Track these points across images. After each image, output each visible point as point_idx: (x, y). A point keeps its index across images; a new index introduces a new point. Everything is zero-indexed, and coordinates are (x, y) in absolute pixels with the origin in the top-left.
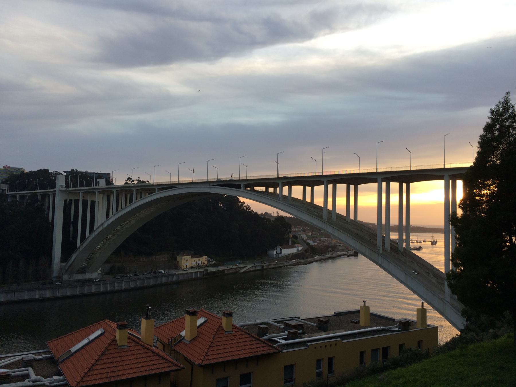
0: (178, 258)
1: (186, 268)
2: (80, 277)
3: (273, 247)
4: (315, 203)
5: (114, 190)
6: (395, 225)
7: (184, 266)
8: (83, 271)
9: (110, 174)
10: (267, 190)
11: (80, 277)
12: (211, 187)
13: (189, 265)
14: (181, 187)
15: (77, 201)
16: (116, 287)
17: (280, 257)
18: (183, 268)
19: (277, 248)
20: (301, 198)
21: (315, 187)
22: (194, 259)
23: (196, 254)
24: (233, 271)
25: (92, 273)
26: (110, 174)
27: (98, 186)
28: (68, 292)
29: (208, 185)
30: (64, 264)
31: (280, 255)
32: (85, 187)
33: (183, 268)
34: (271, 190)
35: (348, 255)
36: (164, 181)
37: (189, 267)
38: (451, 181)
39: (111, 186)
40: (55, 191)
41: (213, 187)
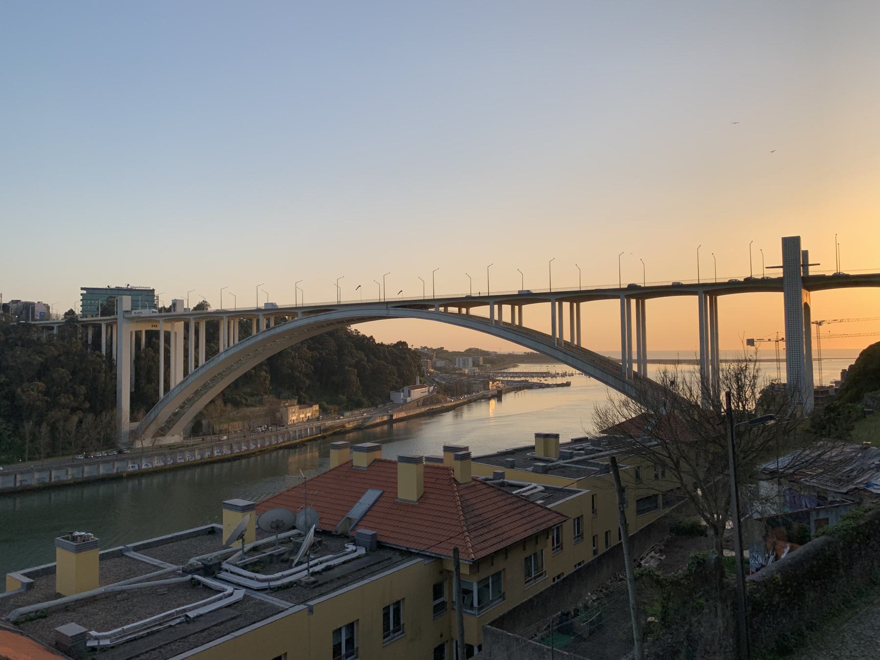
3: (397, 389)
4: (524, 325)
5: (225, 316)
6: (525, 353)
8: (162, 432)
9: (153, 290)
10: (460, 310)
12: (390, 308)
17: (410, 402)
19: (403, 390)
20: (510, 321)
21: (523, 306)
23: (303, 403)
24: (354, 425)
25: (173, 436)
26: (153, 290)
27: (174, 311)
28: (157, 463)
29: (384, 306)
30: (136, 425)
31: (409, 399)
34: (464, 311)
35: (490, 396)
36: (319, 302)
38: (708, 297)
39: (205, 311)
40: (116, 319)
41: (393, 308)
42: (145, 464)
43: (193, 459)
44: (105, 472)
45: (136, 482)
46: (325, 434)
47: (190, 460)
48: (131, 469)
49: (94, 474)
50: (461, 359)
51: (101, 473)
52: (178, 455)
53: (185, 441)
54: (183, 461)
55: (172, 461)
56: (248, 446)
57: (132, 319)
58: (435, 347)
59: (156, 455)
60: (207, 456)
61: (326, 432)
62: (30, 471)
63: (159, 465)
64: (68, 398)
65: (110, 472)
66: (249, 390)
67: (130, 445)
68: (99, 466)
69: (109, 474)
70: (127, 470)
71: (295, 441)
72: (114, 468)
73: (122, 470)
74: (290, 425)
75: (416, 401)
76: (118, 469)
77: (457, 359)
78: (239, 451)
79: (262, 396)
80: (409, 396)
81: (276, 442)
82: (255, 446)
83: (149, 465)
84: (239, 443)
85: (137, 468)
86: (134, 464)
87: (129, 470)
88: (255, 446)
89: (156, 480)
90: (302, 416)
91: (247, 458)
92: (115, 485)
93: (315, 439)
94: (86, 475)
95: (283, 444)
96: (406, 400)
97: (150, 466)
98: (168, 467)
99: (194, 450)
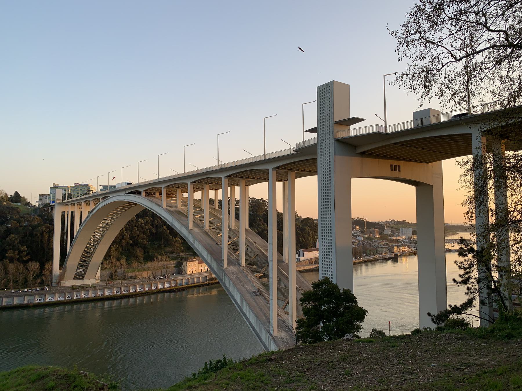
0: (184, 263)
1: (192, 273)
2: (79, 283)
7: (189, 272)
8: (80, 276)
11: (79, 283)
13: (196, 271)
14: (111, 195)
15: (68, 212)
16: (107, 293)
18: (188, 273)
22: (201, 264)
31: (302, 259)
32: (68, 199)
33: (188, 273)
37: (196, 272)
42: (49, 298)
43: (88, 297)
44: (20, 302)
45: (42, 310)
46: (211, 282)
47: (86, 297)
48: (39, 301)
49: (11, 303)
50: (403, 229)
51: (15, 303)
52: (75, 293)
53: (102, 283)
54: (79, 297)
55: (71, 298)
56: (136, 289)
57: (62, 204)
58: (384, 220)
59: (57, 293)
60: (100, 295)
61: (211, 281)
62: (12, 296)
63: (60, 299)
64: (14, 253)
65: (22, 303)
66: (171, 249)
67: (58, 284)
68: (14, 299)
69: (22, 304)
70: (34, 302)
71: (180, 287)
72: (24, 300)
73: (31, 302)
74: (189, 274)
75: (307, 260)
76: (28, 301)
77: (401, 228)
78: (128, 292)
79: (180, 253)
80: (304, 257)
81: (163, 287)
82: (142, 289)
83: (52, 299)
84: (127, 287)
85: (42, 301)
86: (41, 298)
87: (36, 302)
88: (142, 289)
89: (57, 309)
90: (201, 268)
91: (127, 298)
92: (25, 311)
93: (198, 286)
94: (4, 304)
95: (169, 289)
96: (299, 259)
97: (53, 300)
98: (65, 301)
99: (88, 291)
